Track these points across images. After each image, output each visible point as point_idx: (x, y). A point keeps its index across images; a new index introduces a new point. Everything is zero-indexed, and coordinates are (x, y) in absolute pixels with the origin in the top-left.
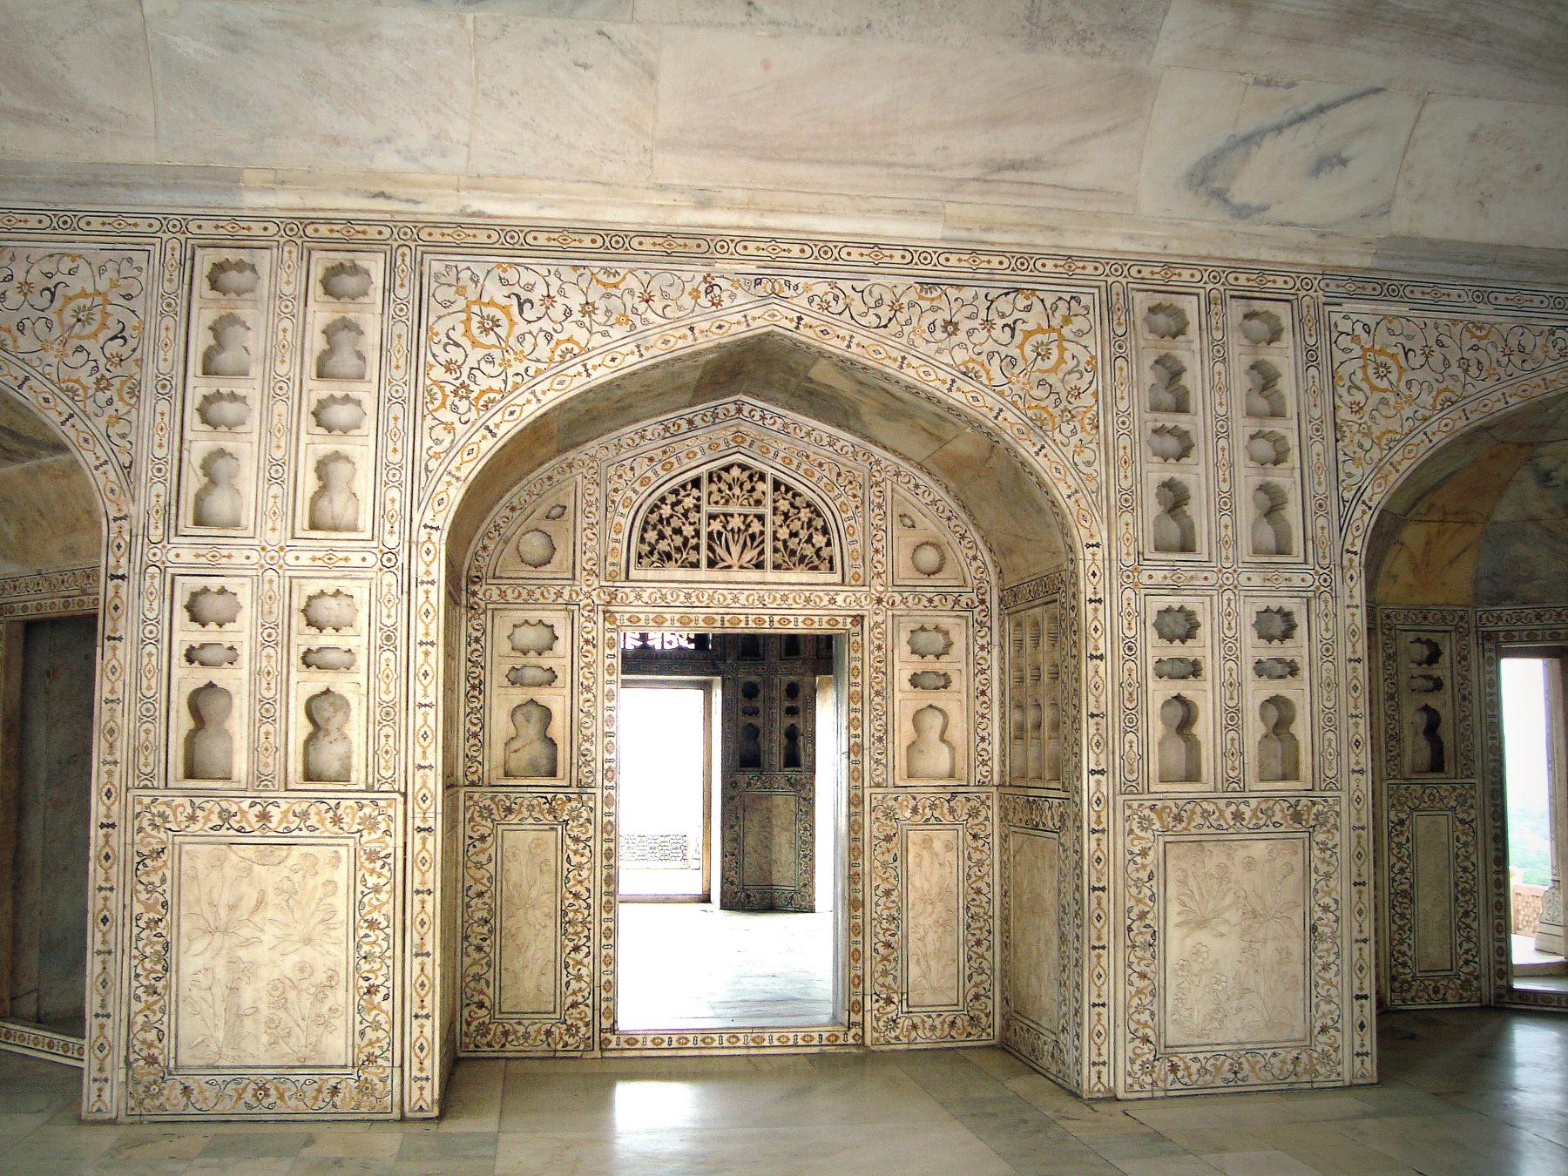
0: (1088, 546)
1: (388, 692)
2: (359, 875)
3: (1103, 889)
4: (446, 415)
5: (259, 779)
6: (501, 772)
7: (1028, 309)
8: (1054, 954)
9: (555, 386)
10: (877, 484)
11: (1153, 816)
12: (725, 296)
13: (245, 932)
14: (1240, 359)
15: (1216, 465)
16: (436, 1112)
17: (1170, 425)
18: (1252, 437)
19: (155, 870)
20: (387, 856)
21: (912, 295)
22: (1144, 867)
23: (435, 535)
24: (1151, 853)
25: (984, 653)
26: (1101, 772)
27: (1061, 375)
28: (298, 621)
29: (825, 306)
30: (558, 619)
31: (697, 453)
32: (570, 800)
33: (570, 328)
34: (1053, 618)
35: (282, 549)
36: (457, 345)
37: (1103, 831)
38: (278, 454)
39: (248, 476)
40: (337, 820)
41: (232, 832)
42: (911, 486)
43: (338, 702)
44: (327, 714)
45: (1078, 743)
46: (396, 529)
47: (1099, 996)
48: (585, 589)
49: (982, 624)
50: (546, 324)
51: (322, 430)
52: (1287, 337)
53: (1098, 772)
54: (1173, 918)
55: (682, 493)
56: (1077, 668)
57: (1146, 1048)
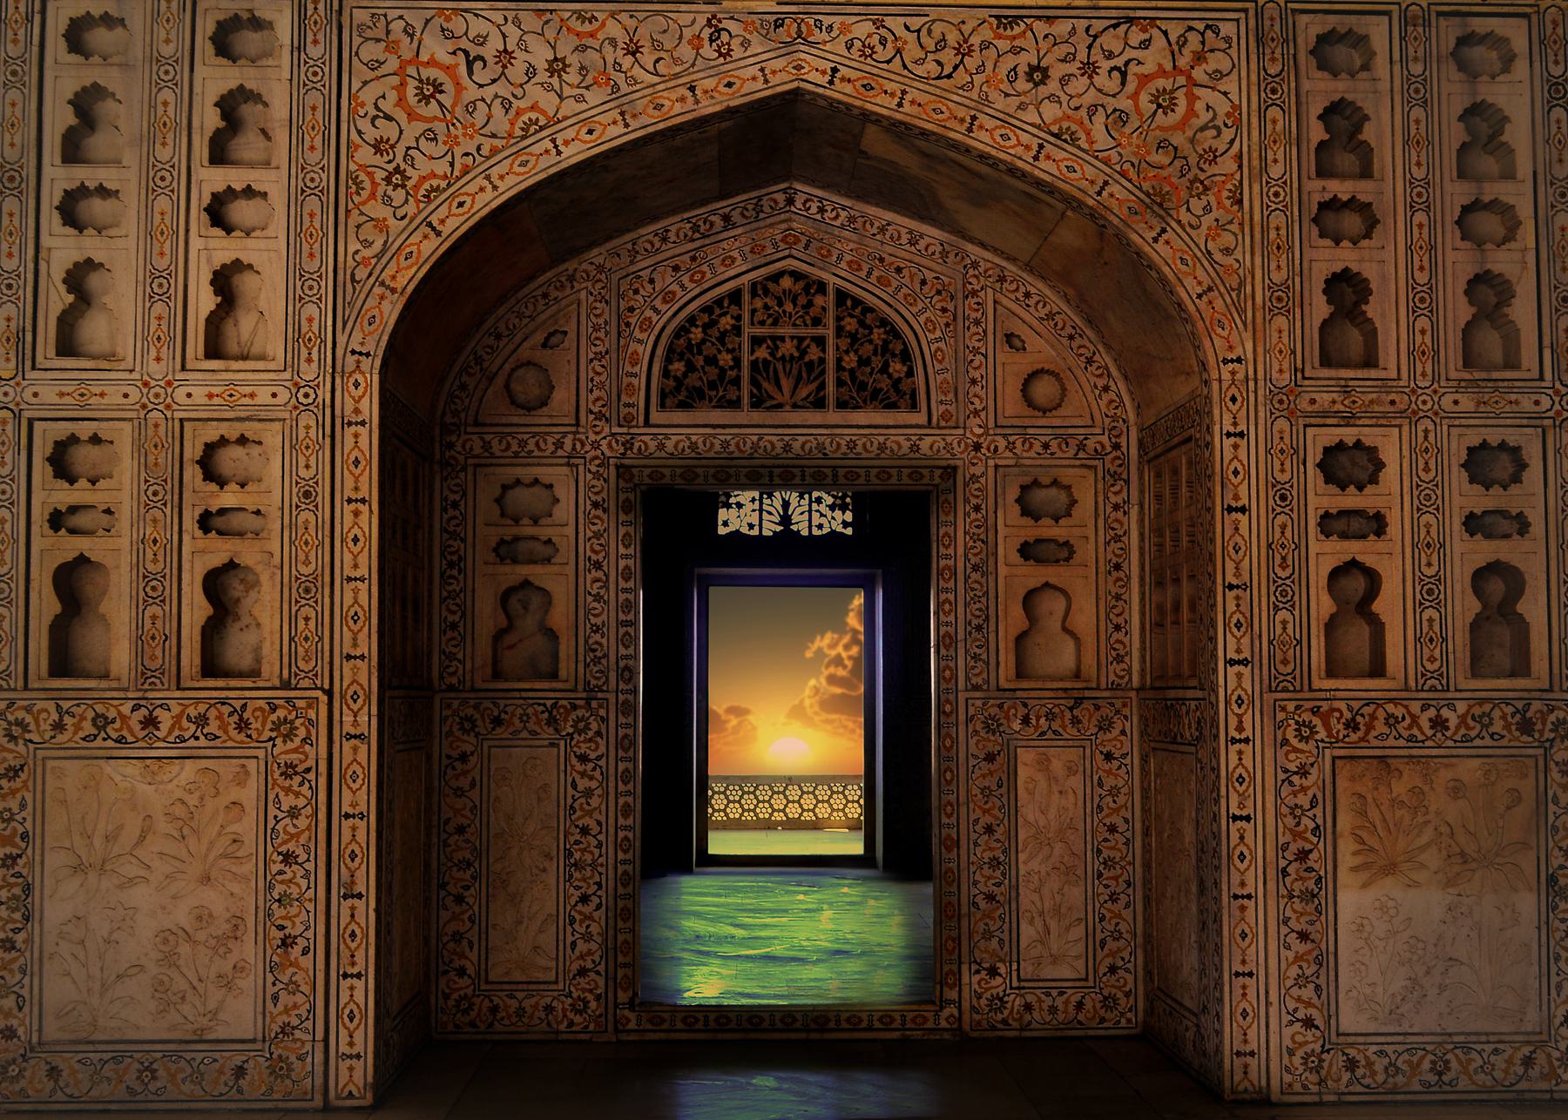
0: (1225, 361)
1: (307, 563)
2: (271, 797)
3: (1248, 818)
4: (377, 210)
5: (145, 675)
6: (489, 671)
7: (1145, 45)
8: (1194, 909)
9: (516, 169)
10: (974, 293)
11: (1316, 721)
12: (735, 43)
13: (132, 870)
14: (1453, 94)
15: (1408, 248)
16: (369, 1099)
17: (1345, 198)
18: (1466, 210)
19: (13, 792)
20: (308, 770)
21: (986, 33)
22: (1304, 789)
23: (366, 363)
24: (1314, 771)
25: (1120, 514)
26: (1244, 662)
27: (1190, 133)
28: (193, 474)
29: (868, 52)
30: (557, 475)
31: (734, 262)
32: (575, 707)
33: (535, 92)
34: (1190, 463)
35: (169, 383)
36: (388, 118)
37: (1247, 740)
38: (162, 263)
39: (121, 294)
40: (242, 725)
41: (110, 743)
42: (1020, 295)
43: (250, 577)
44: (236, 594)
45: (1213, 625)
46: (315, 356)
47: (1244, 962)
48: (592, 437)
49: (1115, 476)
50: (501, 89)
51: (218, 232)
52: (1521, 67)
53: (1239, 662)
54: (1347, 859)
55: (718, 311)
56: (1212, 524)
57: (1310, 1035)
